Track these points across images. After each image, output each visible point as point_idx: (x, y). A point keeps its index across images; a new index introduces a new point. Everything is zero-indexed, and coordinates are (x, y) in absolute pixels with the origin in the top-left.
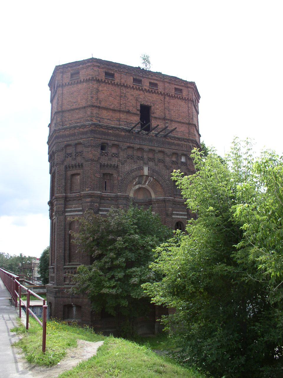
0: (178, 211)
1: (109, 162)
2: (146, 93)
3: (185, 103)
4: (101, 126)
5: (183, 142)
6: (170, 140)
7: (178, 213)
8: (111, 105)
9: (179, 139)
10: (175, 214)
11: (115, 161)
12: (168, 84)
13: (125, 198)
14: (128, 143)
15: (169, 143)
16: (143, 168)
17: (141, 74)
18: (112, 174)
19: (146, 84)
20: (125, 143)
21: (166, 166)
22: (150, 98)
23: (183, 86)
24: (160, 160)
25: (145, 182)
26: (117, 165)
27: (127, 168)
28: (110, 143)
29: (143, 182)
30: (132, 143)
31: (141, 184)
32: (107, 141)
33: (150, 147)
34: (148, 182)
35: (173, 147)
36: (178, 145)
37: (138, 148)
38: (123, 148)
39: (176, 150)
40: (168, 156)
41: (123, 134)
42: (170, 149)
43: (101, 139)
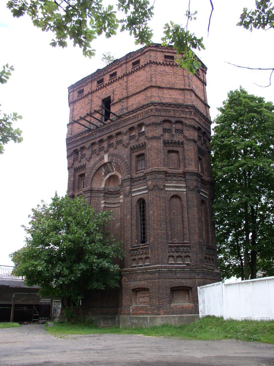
0: (139, 187)
3: (144, 70)
5: (139, 112)
6: (125, 118)
7: (138, 189)
9: (133, 111)
11: (84, 161)
12: (125, 65)
14: (91, 140)
15: (124, 121)
17: (102, 73)
19: (107, 79)
21: (123, 145)
22: (111, 89)
23: (139, 56)
24: (118, 142)
25: (112, 168)
26: (85, 164)
27: (92, 162)
28: (78, 148)
29: (111, 170)
30: (94, 139)
31: (110, 172)
34: (114, 168)
35: (128, 123)
36: (134, 117)
37: (99, 141)
38: (87, 146)
39: (132, 123)
42: (126, 126)
43: (73, 148)
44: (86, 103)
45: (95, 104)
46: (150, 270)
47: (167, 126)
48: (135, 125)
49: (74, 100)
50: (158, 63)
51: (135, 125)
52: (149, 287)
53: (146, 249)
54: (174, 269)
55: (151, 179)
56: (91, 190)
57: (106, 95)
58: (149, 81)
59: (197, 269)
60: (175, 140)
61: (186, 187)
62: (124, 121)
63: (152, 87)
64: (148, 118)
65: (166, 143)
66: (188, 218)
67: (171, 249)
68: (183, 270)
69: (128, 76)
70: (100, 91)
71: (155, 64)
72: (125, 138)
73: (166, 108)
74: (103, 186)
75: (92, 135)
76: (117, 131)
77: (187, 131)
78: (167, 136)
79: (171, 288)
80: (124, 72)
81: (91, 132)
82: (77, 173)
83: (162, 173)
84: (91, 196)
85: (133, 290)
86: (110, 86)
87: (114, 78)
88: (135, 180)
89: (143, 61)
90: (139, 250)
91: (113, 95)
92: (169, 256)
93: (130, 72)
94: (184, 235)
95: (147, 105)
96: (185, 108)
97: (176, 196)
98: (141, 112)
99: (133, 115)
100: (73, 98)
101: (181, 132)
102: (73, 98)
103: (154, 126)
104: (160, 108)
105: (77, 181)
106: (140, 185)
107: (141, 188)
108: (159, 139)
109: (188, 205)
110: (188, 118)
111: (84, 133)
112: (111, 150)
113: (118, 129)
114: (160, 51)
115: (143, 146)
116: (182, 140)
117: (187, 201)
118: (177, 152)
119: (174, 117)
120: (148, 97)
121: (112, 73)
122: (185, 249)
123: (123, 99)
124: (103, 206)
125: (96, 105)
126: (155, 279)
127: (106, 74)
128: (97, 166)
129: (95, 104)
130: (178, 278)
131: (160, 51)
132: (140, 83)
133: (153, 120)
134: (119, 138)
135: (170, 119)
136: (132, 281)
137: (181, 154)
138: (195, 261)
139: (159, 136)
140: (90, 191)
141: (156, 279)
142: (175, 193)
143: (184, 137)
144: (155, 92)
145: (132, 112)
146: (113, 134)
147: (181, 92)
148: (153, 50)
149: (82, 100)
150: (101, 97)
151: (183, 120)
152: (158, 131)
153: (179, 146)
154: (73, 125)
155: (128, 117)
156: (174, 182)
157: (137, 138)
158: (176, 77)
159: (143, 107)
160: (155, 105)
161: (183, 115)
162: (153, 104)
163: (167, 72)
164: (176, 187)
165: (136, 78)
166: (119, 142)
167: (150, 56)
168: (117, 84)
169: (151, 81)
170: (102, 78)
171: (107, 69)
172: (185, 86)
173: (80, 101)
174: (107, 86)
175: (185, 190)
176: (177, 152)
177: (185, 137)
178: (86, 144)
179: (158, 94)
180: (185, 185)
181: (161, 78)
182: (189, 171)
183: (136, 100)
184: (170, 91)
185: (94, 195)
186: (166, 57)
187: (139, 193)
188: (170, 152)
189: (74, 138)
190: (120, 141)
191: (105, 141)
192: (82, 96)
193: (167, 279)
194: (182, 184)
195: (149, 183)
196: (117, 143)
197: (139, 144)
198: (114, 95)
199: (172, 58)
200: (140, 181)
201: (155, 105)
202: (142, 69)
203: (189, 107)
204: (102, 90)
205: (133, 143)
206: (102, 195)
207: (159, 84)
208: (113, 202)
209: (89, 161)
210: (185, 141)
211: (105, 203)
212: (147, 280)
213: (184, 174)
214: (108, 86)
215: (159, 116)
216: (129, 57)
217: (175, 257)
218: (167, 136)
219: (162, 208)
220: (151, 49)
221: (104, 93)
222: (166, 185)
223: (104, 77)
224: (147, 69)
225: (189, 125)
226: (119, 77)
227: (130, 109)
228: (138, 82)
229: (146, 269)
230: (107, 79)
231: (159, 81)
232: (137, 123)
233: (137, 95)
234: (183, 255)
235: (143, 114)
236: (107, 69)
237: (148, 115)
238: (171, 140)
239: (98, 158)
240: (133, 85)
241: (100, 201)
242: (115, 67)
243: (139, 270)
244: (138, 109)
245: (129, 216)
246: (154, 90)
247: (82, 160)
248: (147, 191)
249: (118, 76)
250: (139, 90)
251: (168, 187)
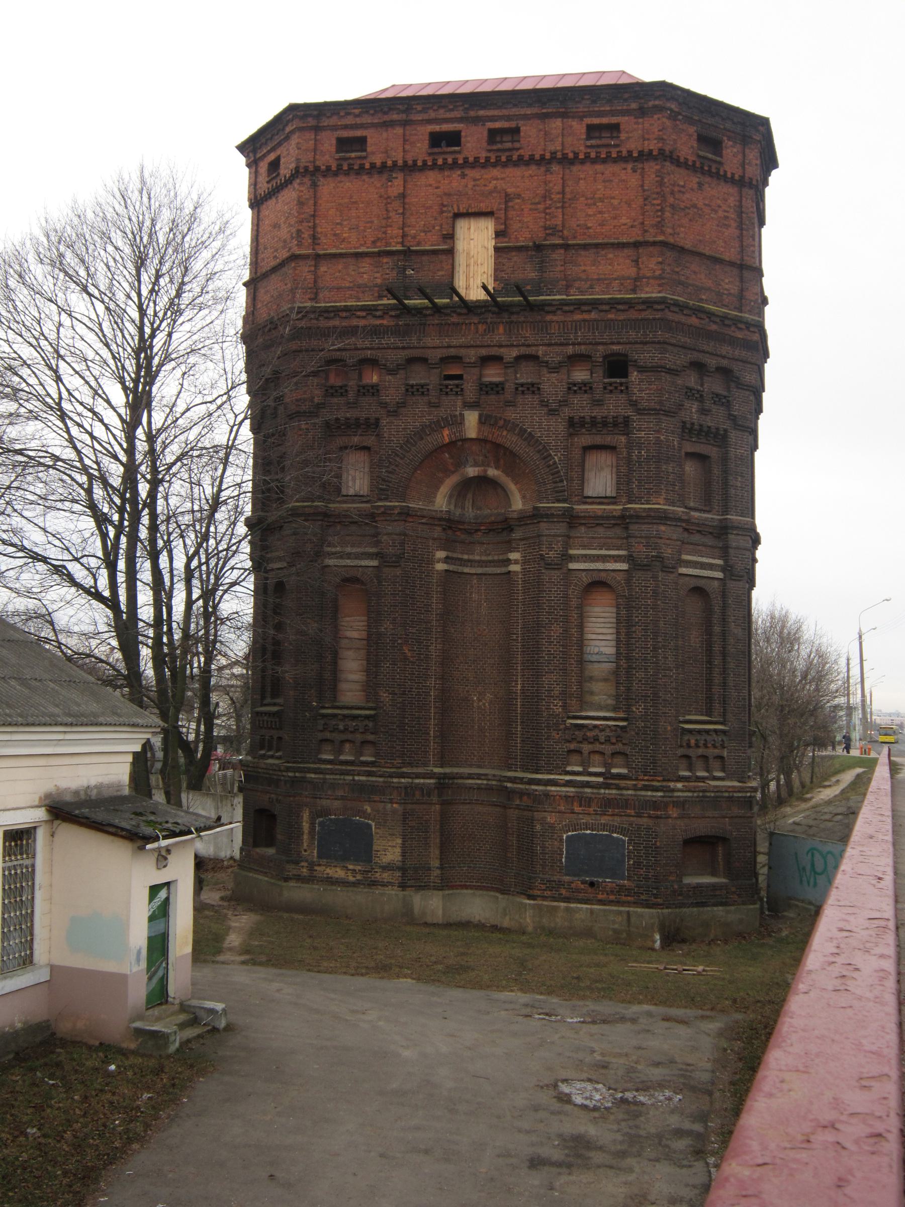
21: (544, 404)
50: (682, 160)
60: (710, 424)
71: (672, 163)
72: (553, 385)
97: (699, 591)
115: (615, 425)
166: (533, 388)
205: (581, 406)
251: (689, 564)
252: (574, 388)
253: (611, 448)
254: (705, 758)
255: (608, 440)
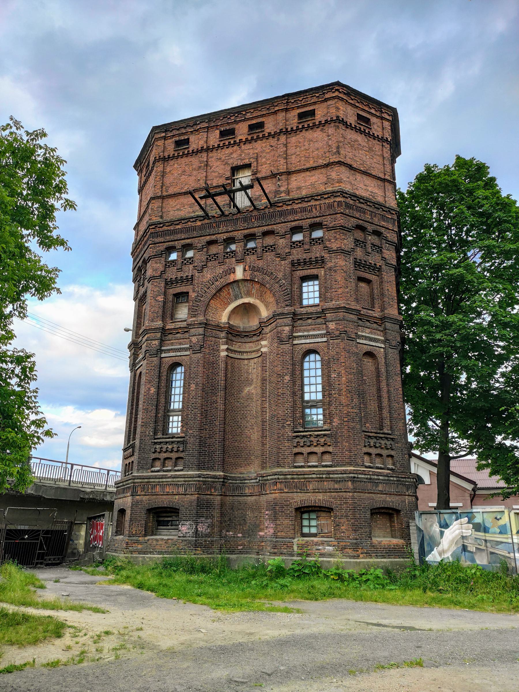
0: (308, 331)
1: (179, 275)
2: (243, 146)
3: (322, 130)
4: (164, 224)
5: (313, 203)
6: (285, 208)
7: (306, 333)
8: (182, 188)
9: (302, 199)
10: (301, 336)
12: (284, 114)
13: (200, 324)
15: (282, 214)
16: (234, 269)
17: (232, 118)
18: (188, 293)
19: (242, 130)
20: (203, 238)
21: (278, 255)
22: (251, 151)
23: (315, 103)
24: (266, 247)
26: (192, 276)
27: (208, 275)
30: (214, 235)
32: (173, 243)
33: (246, 232)
35: (290, 218)
36: (304, 210)
37: (224, 240)
38: (199, 246)
39: (298, 220)
40: (283, 236)
41: (199, 223)
43: (164, 242)
44: (194, 166)
45: (214, 172)
46: (336, 476)
47: (359, 235)
48: (305, 224)
49: (166, 154)
51: (305, 224)
52: (334, 506)
53: (325, 437)
54: (375, 477)
55: (337, 320)
56: (206, 324)
57: (242, 160)
58: (335, 153)
59: (407, 480)
60: (370, 262)
61: (384, 342)
62: (282, 214)
63: (340, 163)
64: (332, 216)
65: (358, 264)
66: (388, 391)
67: (369, 442)
68: (388, 480)
69: (289, 136)
70: (227, 151)
71: (344, 125)
73: (359, 205)
74: (224, 318)
75: (210, 226)
76: (265, 228)
77: (388, 250)
78: (359, 253)
79: (371, 510)
80: (281, 126)
81: (206, 221)
82: (171, 290)
83: (353, 313)
84: (204, 335)
85: (297, 509)
86: (248, 146)
87: (259, 132)
88: (299, 317)
89: (321, 113)
90: (312, 439)
91: (255, 163)
92: (365, 453)
93: (295, 128)
94: (381, 419)
95: (333, 194)
96: (386, 211)
97: (370, 354)
98: (318, 203)
99: (300, 205)
100: (163, 152)
101: (379, 249)
102: (163, 152)
103: (342, 231)
104: (351, 202)
105: (170, 305)
106: (309, 328)
107: (311, 333)
108: (348, 256)
109: (387, 371)
110: (390, 229)
111: (191, 220)
112: (251, 259)
113: (268, 225)
114: (351, 104)
115: (317, 262)
116: (380, 264)
117: (387, 365)
118: (368, 282)
119: (370, 223)
120: (333, 180)
121: (254, 122)
122: (388, 443)
123: (281, 174)
124: (224, 354)
125: (217, 174)
126: (345, 492)
127: (240, 121)
128: (217, 283)
129: (214, 172)
130: (381, 493)
131: (351, 104)
132: (313, 152)
133: (341, 220)
134: (269, 240)
135: (366, 225)
136: (297, 492)
137: (376, 285)
138: (401, 465)
139: (349, 250)
140: (204, 326)
141: (349, 492)
142: (369, 349)
143: (382, 260)
144: (344, 173)
145: (300, 201)
146: (258, 231)
147: (380, 183)
148: (342, 99)
149: (184, 160)
150: (230, 161)
151: (383, 230)
152: (348, 243)
153: (373, 273)
154: (165, 201)
155: (289, 208)
156: (368, 330)
157: (307, 247)
158: (373, 156)
159: (322, 195)
160: (346, 195)
161: (384, 223)
162: (343, 193)
163: (360, 145)
164: (371, 339)
165: (305, 141)
166: (272, 248)
167: (338, 109)
168: (264, 145)
169: (338, 152)
170: (231, 126)
171: (244, 113)
172: (385, 174)
173: (180, 160)
174: (242, 144)
175: (383, 346)
176: (368, 282)
177: (384, 259)
178: (196, 240)
179: (348, 178)
180: (383, 338)
181: (352, 152)
182: (391, 316)
183: (305, 181)
184: (365, 177)
185: (209, 333)
186: (359, 117)
187: (308, 341)
188: (361, 279)
189: (167, 224)
190: (271, 246)
191: (240, 241)
192: (186, 152)
193: (366, 493)
194: (378, 335)
195: (332, 326)
196: (263, 250)
197: (311, 258)
198: (257, 163)
199: (367, 121)
200: (310, 321)
201: (346, 195)
202: (320, 129)
203: (392, 212)
204: (230, 150)
205: (298, 254)
206: (223, 335)
207: (349, 161)
208: (239, 350)
209: (201, 271)
210: (384, 267)
211: (228, 350)
212: (329, 492)
213: (383, 319)
214: (244, 144)
215: (351, 216)
216: (293, 101)
217: (373, 456)
218: (359, 253)
219: (353, 371)
220: (341, 95)
221: (234, 155)
222: (359, 333)
223: (236, 126)
224: (331, 130)
225: (391, 242)
226: (269, 133)
227: (294, 195)
228: (311, 150)
229: (329, 473)
230: (242, 130)
231: (347, 155)
232: (309, 221)
233: (308, 173)
234: (319, 450)
235: (320, 207)
236: (244, 113)
237: (332, 212)
238: (365, 261)
239: (220, 270)
240: (298, 153)
241: (218, 345)
242: (262, 113)
243: (314, 474)
244: (312, 197)
245: (287, 378)
246: (343, 169)
247: (185, 268)
248: (325, 339)
249: (268, 131)
250: (311, 164)
252: (294, 245)
253: (314, 277)
254: (380, 455)
255: (314, 272)
